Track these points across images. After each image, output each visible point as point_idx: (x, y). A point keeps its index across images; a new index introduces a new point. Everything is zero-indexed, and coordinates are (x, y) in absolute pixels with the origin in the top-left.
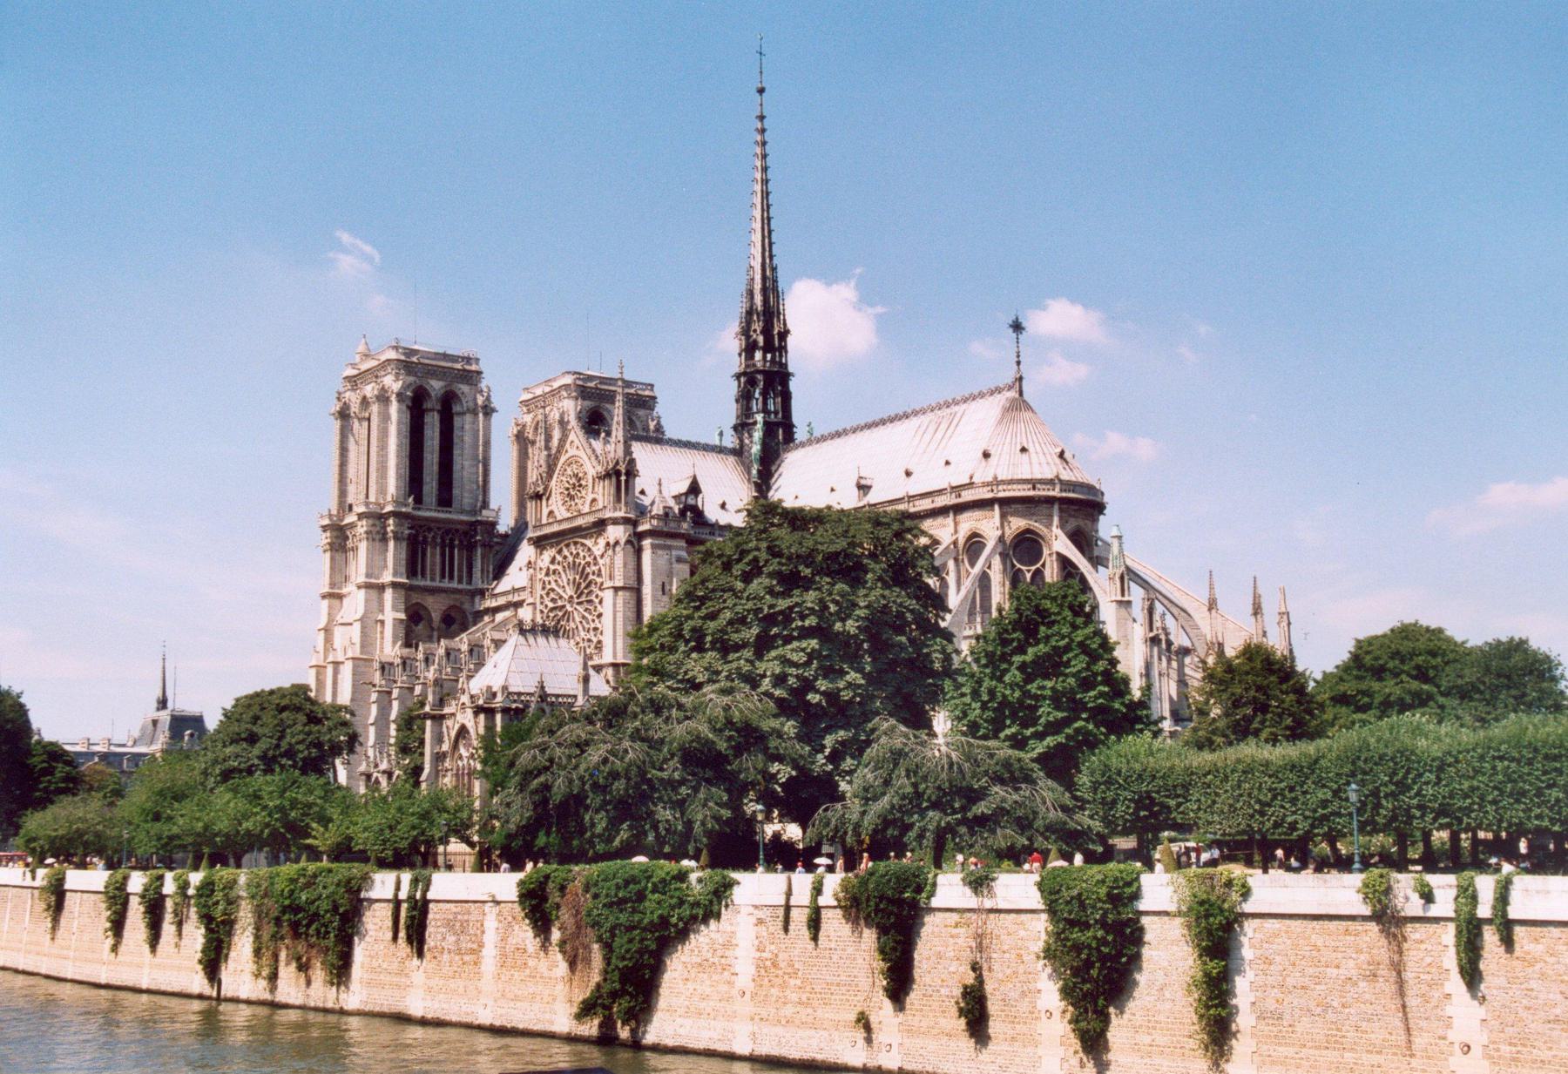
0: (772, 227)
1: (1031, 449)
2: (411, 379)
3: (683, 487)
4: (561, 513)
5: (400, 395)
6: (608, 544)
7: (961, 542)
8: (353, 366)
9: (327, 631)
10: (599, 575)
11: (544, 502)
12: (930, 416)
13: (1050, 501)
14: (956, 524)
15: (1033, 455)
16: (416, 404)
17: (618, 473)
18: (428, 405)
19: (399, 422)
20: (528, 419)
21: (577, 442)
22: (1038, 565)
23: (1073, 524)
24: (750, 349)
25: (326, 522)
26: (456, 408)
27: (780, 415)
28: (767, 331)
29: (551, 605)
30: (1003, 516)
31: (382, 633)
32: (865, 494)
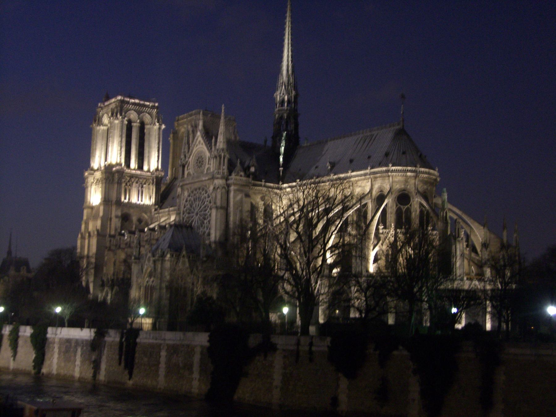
6: (214, 188)
7: (374, 193)
9: (87, 224)
10: (210, 202)
11: (186, 169)
21: (202, 141)
22: (409, 206)
29: (187, 215)
31: (110, 224)
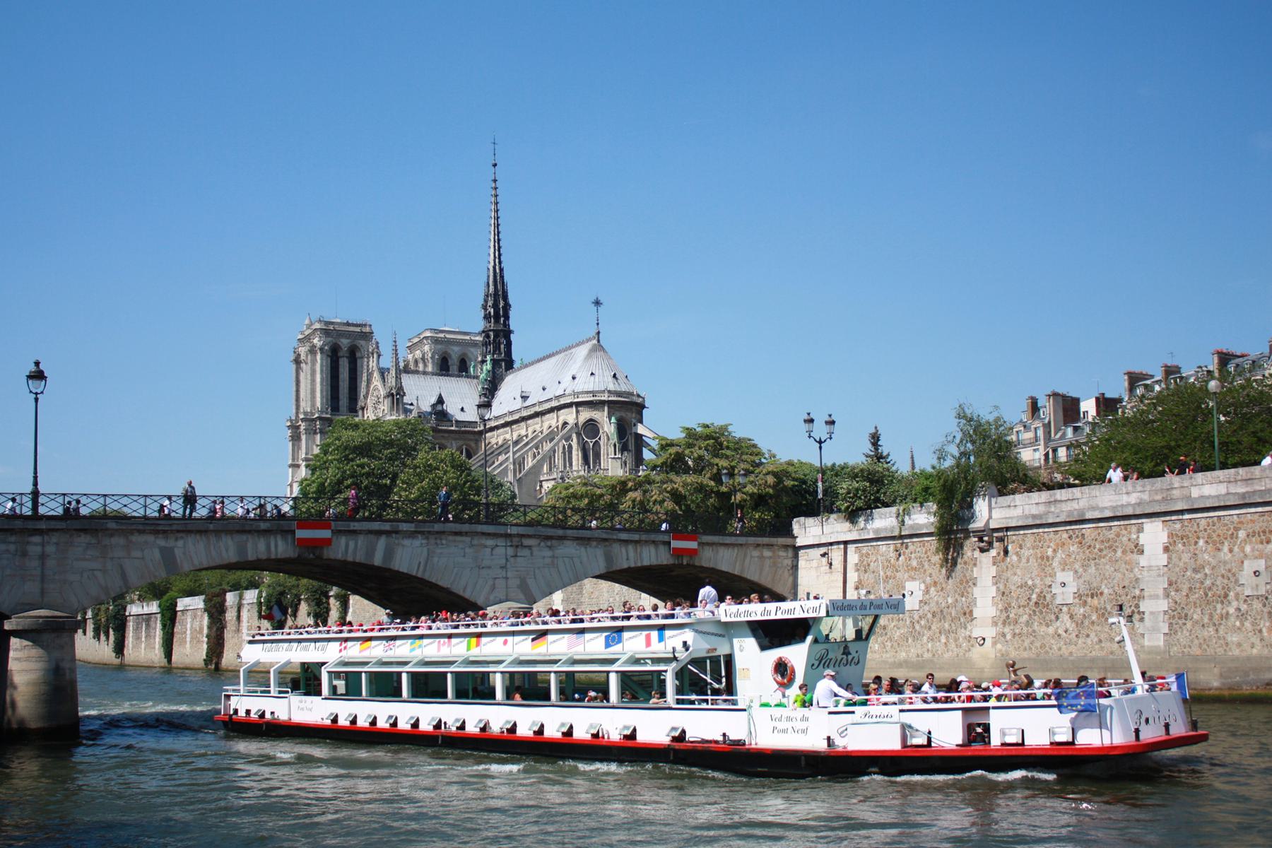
0: (501, 245)
1: (597, 374)
2: (330, 339)
3: (433, 400)
4: (372, 417)
5: (321, 349)
7: (560, 427)
8: (302, 333)
12: (563, 354)
13: (603, 403)
14: (558, 417)
15: (597, 377)
16: (333, 355)
17: (392, 394)
18: (340, 354)
19: (322, 366)
20: (410, 357)
23: (618, 414)
24: (487, 317)
25: (289, 424)
26: (358, 355)
27: (503, 355)
28: (495, 306)
30: (577, 412)
32: (525, 401)
